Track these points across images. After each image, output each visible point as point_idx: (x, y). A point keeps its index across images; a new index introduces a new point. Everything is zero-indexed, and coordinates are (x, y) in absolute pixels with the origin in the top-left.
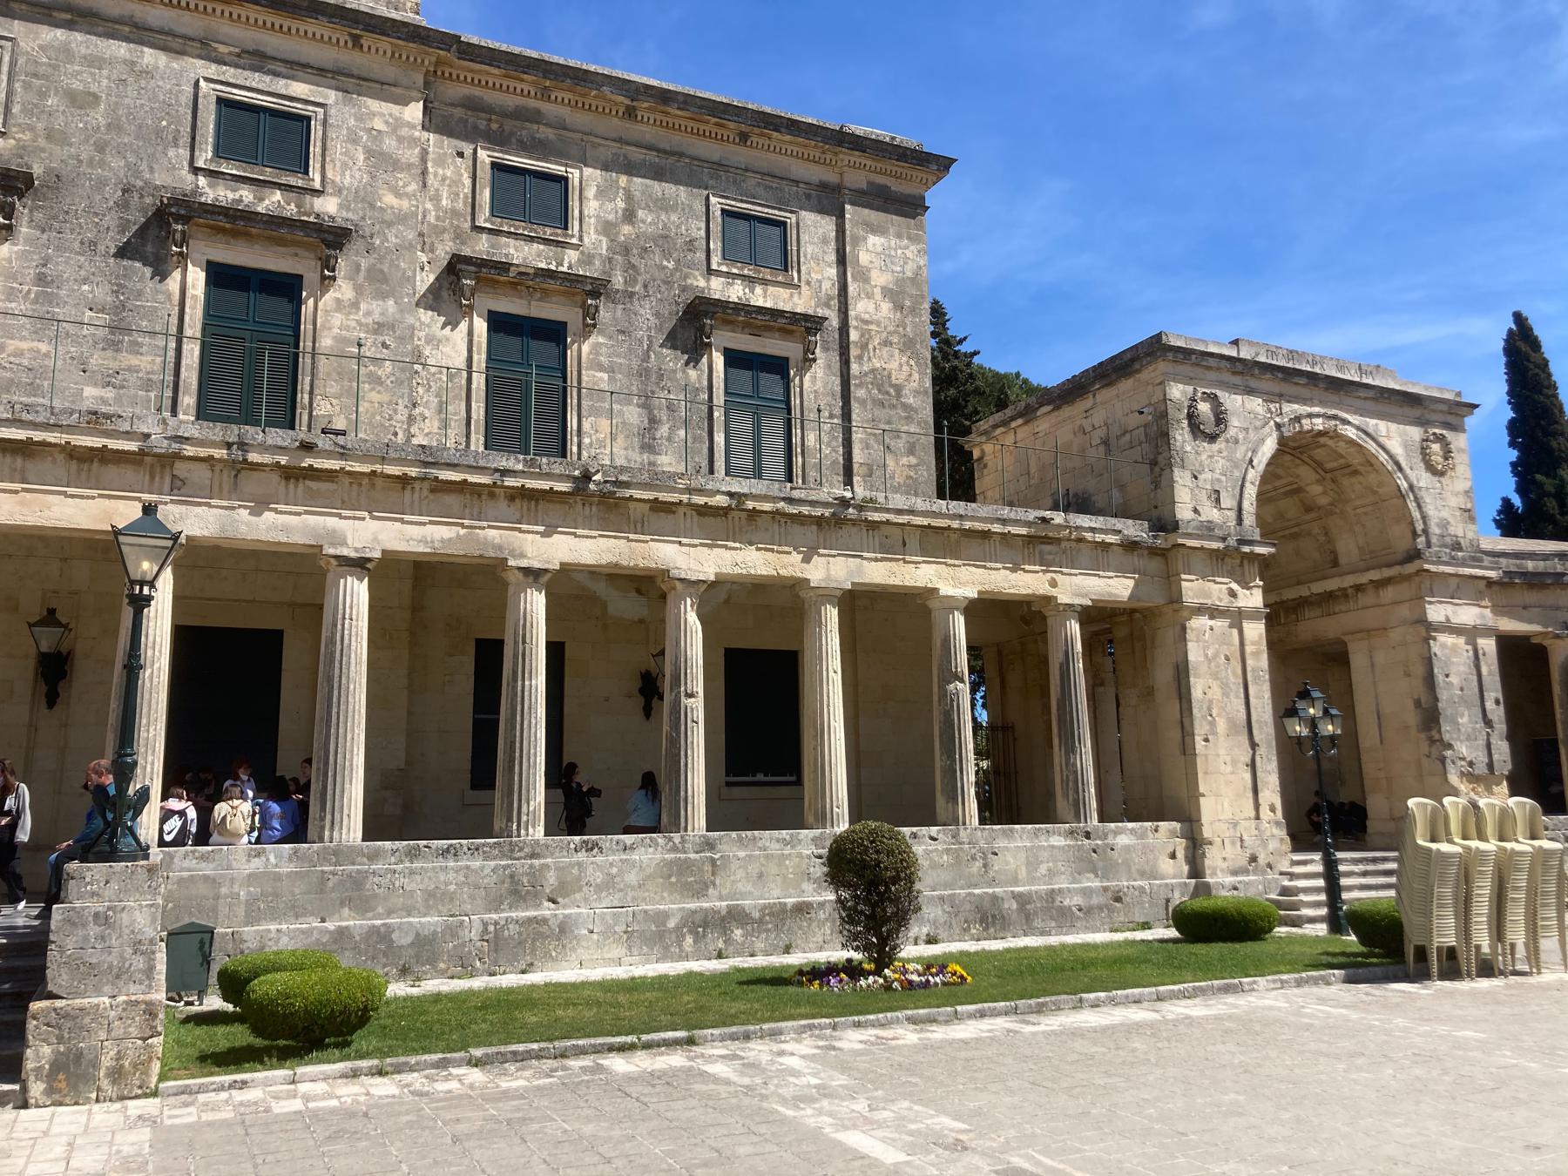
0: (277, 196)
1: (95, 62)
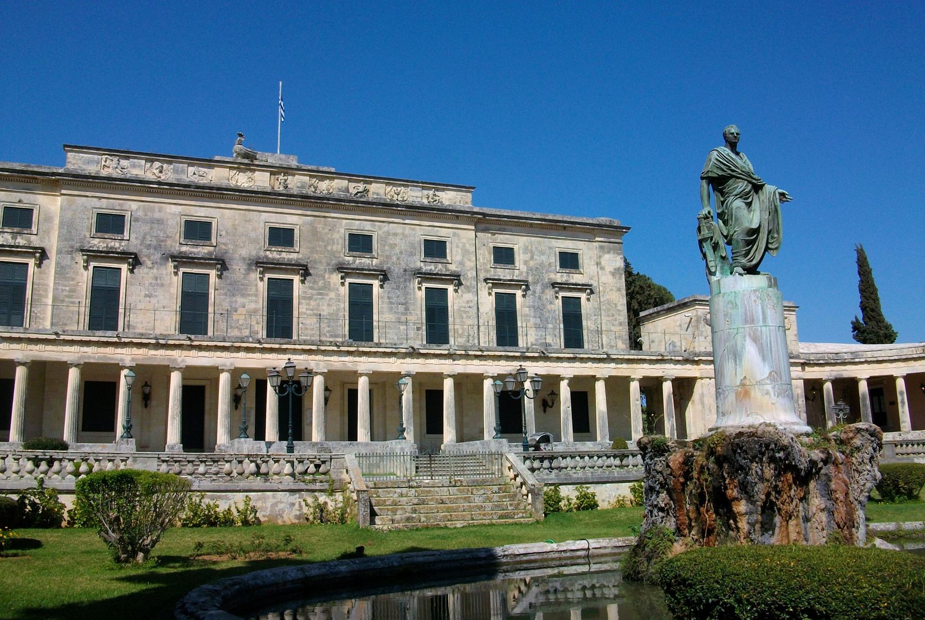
0: (440, 266)
1: (395, 234)
